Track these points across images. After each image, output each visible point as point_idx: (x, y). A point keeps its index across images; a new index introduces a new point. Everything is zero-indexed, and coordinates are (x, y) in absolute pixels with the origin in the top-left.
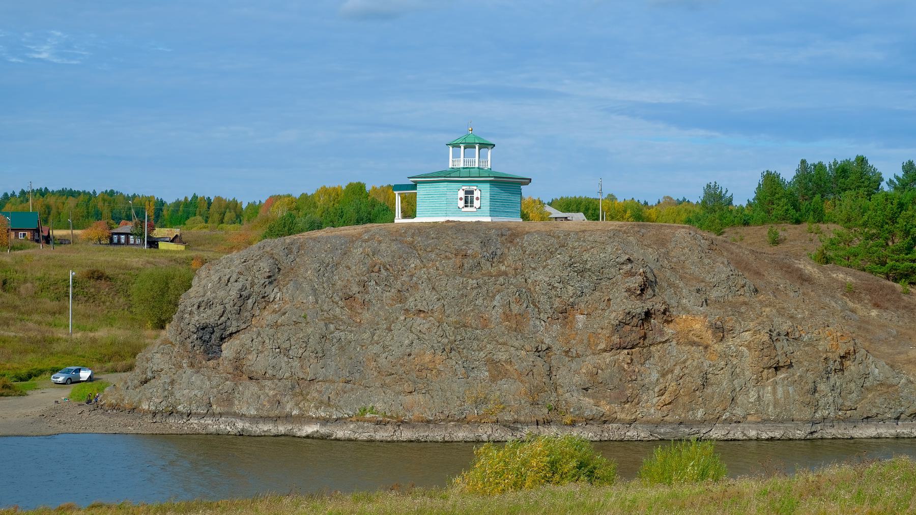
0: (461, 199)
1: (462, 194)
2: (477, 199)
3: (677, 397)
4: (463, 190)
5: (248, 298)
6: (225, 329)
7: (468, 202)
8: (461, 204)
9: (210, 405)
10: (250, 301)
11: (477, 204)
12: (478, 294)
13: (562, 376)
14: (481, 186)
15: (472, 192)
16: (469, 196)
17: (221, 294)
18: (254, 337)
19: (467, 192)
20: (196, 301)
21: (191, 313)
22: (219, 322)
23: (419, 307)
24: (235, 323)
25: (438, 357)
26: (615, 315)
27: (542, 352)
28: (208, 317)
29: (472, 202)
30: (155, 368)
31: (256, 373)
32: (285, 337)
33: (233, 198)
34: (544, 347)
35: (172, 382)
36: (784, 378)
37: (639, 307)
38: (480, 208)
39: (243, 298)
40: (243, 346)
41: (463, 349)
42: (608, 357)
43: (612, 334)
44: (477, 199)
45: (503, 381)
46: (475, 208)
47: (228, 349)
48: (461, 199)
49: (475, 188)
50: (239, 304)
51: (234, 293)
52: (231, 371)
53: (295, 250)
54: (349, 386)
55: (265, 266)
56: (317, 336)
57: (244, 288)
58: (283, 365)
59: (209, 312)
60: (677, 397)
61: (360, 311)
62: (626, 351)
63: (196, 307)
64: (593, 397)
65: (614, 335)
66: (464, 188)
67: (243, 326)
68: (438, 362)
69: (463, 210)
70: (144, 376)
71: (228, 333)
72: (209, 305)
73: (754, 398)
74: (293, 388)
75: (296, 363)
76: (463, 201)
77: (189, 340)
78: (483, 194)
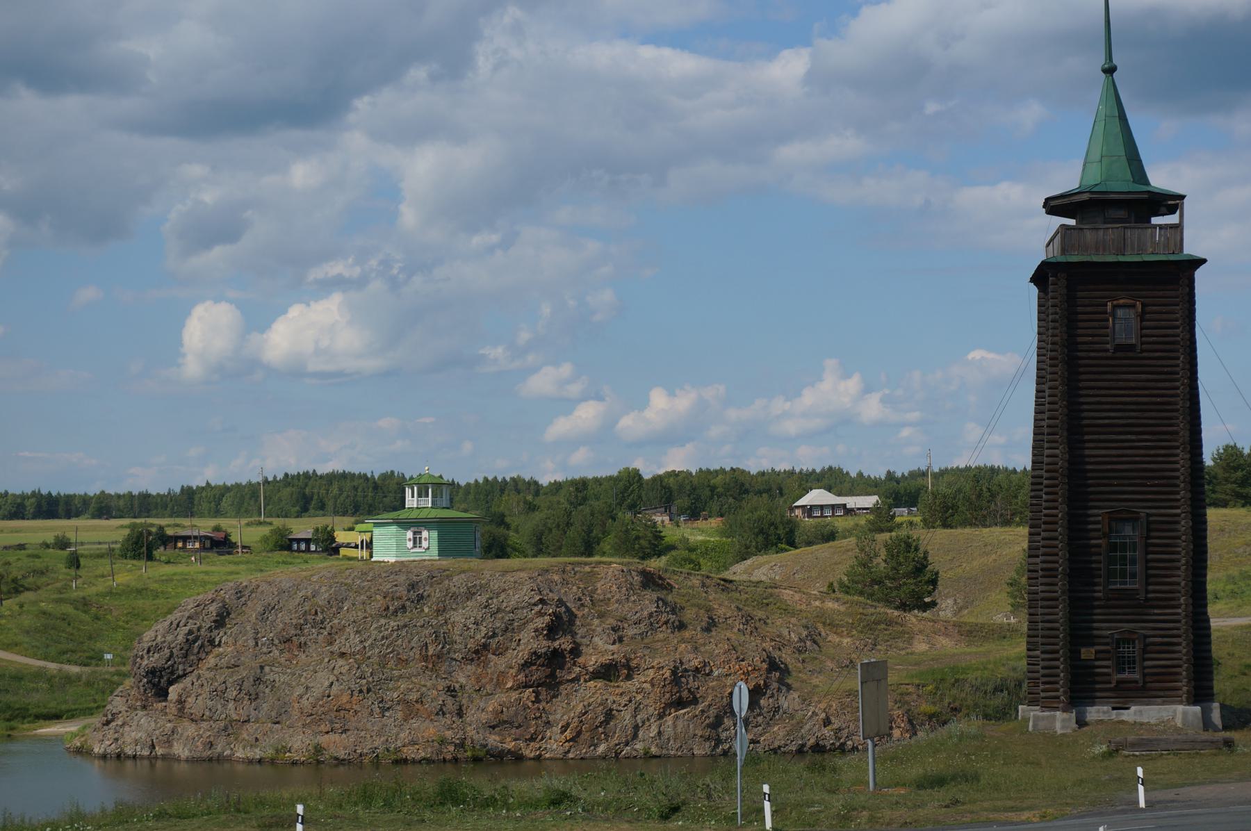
0: (410, 540)
2: (425, 539)
3: (579, 733)
5: (195, 641)
6: (172, 673)
8: (410, 544)
9: (153, 746)
10: (197, 644)
11: (425, 544)
18: (195, 680)
19: (415, 533)
20: (146, 646)
21: (142, 658)
22: (166, 666)
23: (343, 650)
24: (181, 667)
25: (355, 698)
26: (521, 654)
28: (155, 660)
29: (420, 543)
30: (114, 711)
31: (196, 715)
32: (222, 679)
35: (123, 725)
36: (685, 713)
37: (543, 645)
38: (428, 548)
39: (189, 643)
40: (184, 689)
41: (380, 689)
42: (514, 695)
43: (519, 671)
44: (425, 539)
45: (414, 721)
47: (174, 691)
48: (410, 540)
49: (423, 528)
50: (186, 648)
52: (176, 714)
53: (247, 593)
57: (190, 632)
58: (219, 706)
59: (156, 655)
60: (579, 733)
61: (296, 653)
62: (531, 690)
63: (145, 651)
65: (520, 674)
67: (190, 669)
68: (354, 702)
69: (412, 551)
70: (105, 719)
72: (158, 649)
73: (654, 733)
74: (225, 729)
75: (231, 705)
76: (412, 542)
77: (141, 684)
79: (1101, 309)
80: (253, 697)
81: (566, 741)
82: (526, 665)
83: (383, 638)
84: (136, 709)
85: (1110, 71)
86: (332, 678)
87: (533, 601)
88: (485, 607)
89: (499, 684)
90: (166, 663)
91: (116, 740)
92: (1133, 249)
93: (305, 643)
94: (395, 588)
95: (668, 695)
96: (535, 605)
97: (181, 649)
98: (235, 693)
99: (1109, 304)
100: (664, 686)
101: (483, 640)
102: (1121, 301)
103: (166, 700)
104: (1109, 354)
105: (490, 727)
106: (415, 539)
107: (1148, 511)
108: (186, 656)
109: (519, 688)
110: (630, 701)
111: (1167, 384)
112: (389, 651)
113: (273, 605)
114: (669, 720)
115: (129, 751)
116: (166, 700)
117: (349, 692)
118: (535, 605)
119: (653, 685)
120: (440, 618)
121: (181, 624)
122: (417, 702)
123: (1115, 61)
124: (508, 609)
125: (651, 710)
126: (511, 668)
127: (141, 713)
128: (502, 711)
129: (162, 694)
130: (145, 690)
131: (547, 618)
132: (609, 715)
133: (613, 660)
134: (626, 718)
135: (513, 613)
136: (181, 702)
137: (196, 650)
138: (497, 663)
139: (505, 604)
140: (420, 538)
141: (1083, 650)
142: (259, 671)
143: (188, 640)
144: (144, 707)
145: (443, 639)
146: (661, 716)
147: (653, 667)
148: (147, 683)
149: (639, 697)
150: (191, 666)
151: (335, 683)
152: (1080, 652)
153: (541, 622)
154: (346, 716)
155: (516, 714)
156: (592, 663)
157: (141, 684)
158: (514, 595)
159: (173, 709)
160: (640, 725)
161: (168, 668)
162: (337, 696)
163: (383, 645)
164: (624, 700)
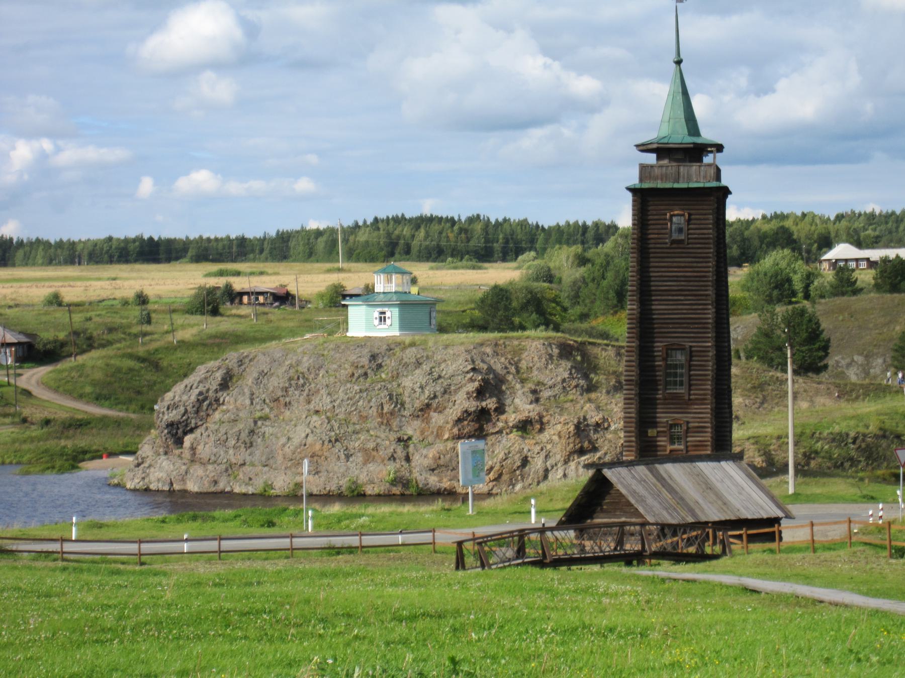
1: (377, 315)
2: (389, 318)
3: (500, 475)
6: (186, 425)
7: (382, 319)
8: (377, 322)
9: (171, 484)
10: (205, 403)
11: (388, 322)
12: (360, 398)
13: (417, 459)
14: (392, 309)
15: (384, 313)
17: (185, 398)
18: (203, 432)
21: (163, 413)
23: (317, 408)
24: (193, 421)
25: (325, 446)
27: (404, 441)
28: (173, 416)
30: (143, 456)
32: (224, 431)
34: (406, 437)
35: (150, 466)
37: (473, 405)
38: (391, 325)
39: (200, 402)
42: (450, 445)
45: (371, 465)
47: (188, 440)
48: (376, 318)
50: (196, 406)
51: (193, 398)
53: (247, 360)
54: (266, 469)
55: (219, 375)
56: (247, 431)
57: (201, 393)
58: (222, 453)
59: (174, 412)
60: (500, 475)
61: (283, 410)
64: (438, 475)
67: (200, 423)
71: (189, 428)
74: (227, 470)
75: (231, 452)
77: (163, 434)
78: (393, 314)
79: (663, 217)
80: (248, 445)
81: (491, 481)
82: (459, 420)
83: (348, 399)
84: (159, 455)
85: (679, 62)
86: (308, 431)
87: (466, 370)
88: (429, 374)
89: (439, 436)
90: (182, 417)
91: (143, 478)
92: (684, 178)
93: (290, 403)
94: (359, 359)
95: (572, 445)
96: (468, 372)
97: (193, 407)
98: (233, 442)
99: (668, 214)
100: (569, 437)
101: (426, 401)
102: (676, 212)
103: (182, 447)
104: (668, 246)
105: (430, 470)
106: (381, 318)
107: (691, 344)
108: (197, 412)
109: (454, 439)
110: (542, 449)
111: (704, 265)
112: (353, 409)
113: (265, 371)
114: (572, 465)
115: (153, 487)
116: (182, 447)
117: (321, 442)
118: (468, 372)
119: (560, 437)
120: (394, 383)
121: (194, 387)
122: (373, 450)
123: (682, 56)
124: (446, 376)
125: (558, 457)
126: (447, 423)
127: (163, 457)
128: (440, 458)
129: (179, 442)
130: (166, 439)
131: (476, 384)
132: (525, 462)
133: (529, 417)
134: (537, 464)
136: (193, 449)
137: (205, 408)
138: (436, 419)
139: (444, 372)
140: (385, 317)
141: (650, 431)
142: (252, 425)
143: (198, 400)
144: (166, 453)
145: (397, 400)
146: (566, 462)
147: (560, 423)
148: (168, 433)
149: (549, 447)
150: (201, 420)
151: (311, 435)
152: (647, 432)
153: (472, 387)
154: (319, 461)
155: (451, 460)
156: (512, 419)
157: (163, 434)
158: (452, 365)
159: (187, 454)
160: (550, 468)
161: (183, 422)
162: (311, 445)
163: (348, 405)
164: (538, 448)
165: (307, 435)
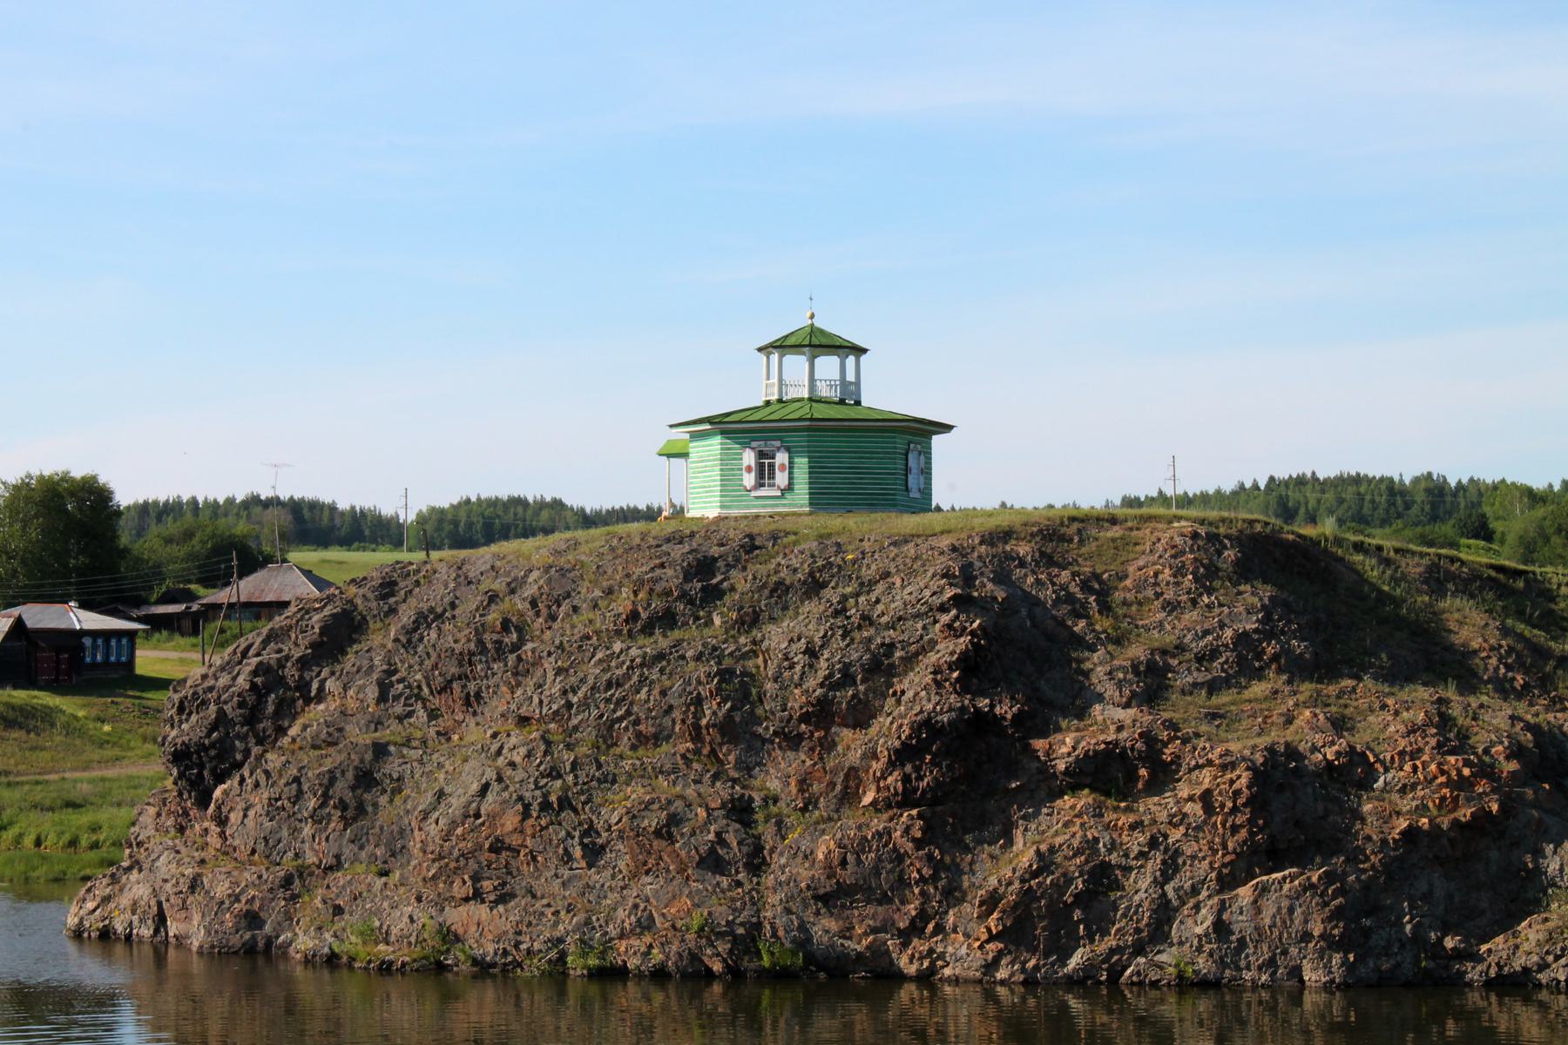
0: (749, 469)
4: (753, 449)
11: (781, 479)
16: (767, 461)
19: (761, 455)
23: (523, 711)
29: (772, 476)
33: (1457, 480)
36: (1284, 878)
37: (945, 705)
41: (585, 803)
44: (782, 468)
46: (779, 487)
48: (749, 469)
49: (778, 444)
58: (285, 833)
65: (891, 774)
66: (754, 444)
68: (529, 831)
69: (754, 494)
73: (1205, 925)
80: (350, 813)
81: (991, 938)
82: (901, 755)
83: (609, 685)
86: (490, 774)
87: (937, 601)
88: (837, 613)
89: (849, 797)
90: (209, 735)
93: (478, 695)
94: (658, 572)
95: (1243, 833)
96: (943, 609)
97: (241, 705)
98: (312, 803)
100: (1234, 810)
101: (819, 691)
105: (816, 898)
106: (761, 467)
109: (889, 806)
110: (1153, 843)
112: (619, 713)
113: (439, 610)
114: (1245, 893)
117: (519, 807)
118: (943, 609)
119: (1209, 808)
120: (742, 640)
121: (251, 652)
122: (658, 833)
124: (884, 619)
126: (875, 756)
128: (844, 863)
131: (964, 641)
133: (1116, 743)
134: (1140, 887)
135: (895, 630)
137: (270, 709)
138: (851, 744)
139: (880, 607)
140: (772, 466)
142: (369, 756)
143: (254, 686)
146: (1228, 882)
147: (1210, 763)
149: (1176, 835)
151: (495, 787)
153: (948, 649)
154: (513, 862)
155: (876, 871)
156: (1064, 750)
158: (903, 587)
160: (1175, 903)
161: (213, 745)
162: (493, 816)
163: (608, 701)
164: (1140, 839)
165: (485, 789)
